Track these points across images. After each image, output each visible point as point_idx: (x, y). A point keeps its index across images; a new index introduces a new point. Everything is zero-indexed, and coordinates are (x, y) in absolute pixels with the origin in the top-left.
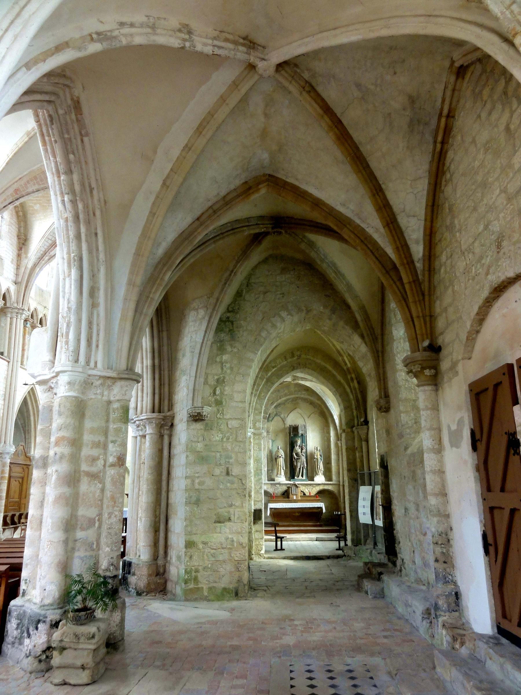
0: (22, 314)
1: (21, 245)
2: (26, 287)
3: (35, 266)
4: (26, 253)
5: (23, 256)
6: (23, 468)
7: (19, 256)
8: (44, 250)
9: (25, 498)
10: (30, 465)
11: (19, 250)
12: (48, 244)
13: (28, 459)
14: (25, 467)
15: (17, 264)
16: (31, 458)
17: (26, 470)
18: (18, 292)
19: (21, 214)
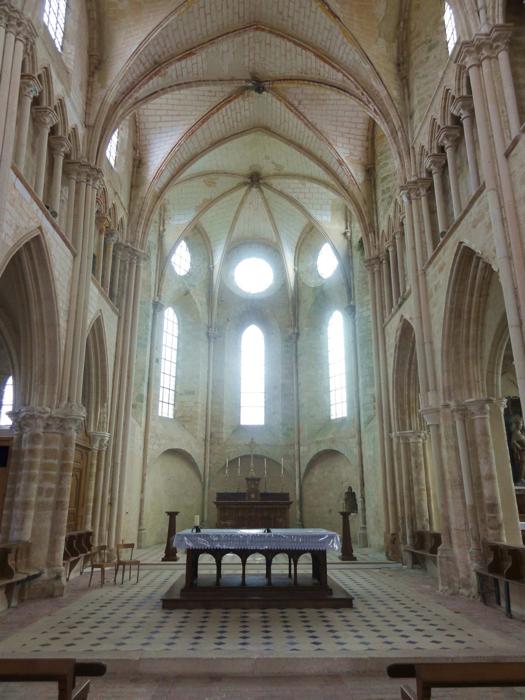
0: (95, 179)
1: (93, 69)
2: (102, 137)
3: (117, 104)
4: (103, 81)
5: (97, 85)
6: (82, 455)
7: (90, 84)
8: (131, 80)
9: (83, 506)
10: (89, 449)
11: (89, 76)
12: (138, 72)
13: (88, 439)
14: (84, 452)
15: (87, 97)
16: (91, 438)
17: (85, 456)
18: (90, 142)
19: (95, 15)
